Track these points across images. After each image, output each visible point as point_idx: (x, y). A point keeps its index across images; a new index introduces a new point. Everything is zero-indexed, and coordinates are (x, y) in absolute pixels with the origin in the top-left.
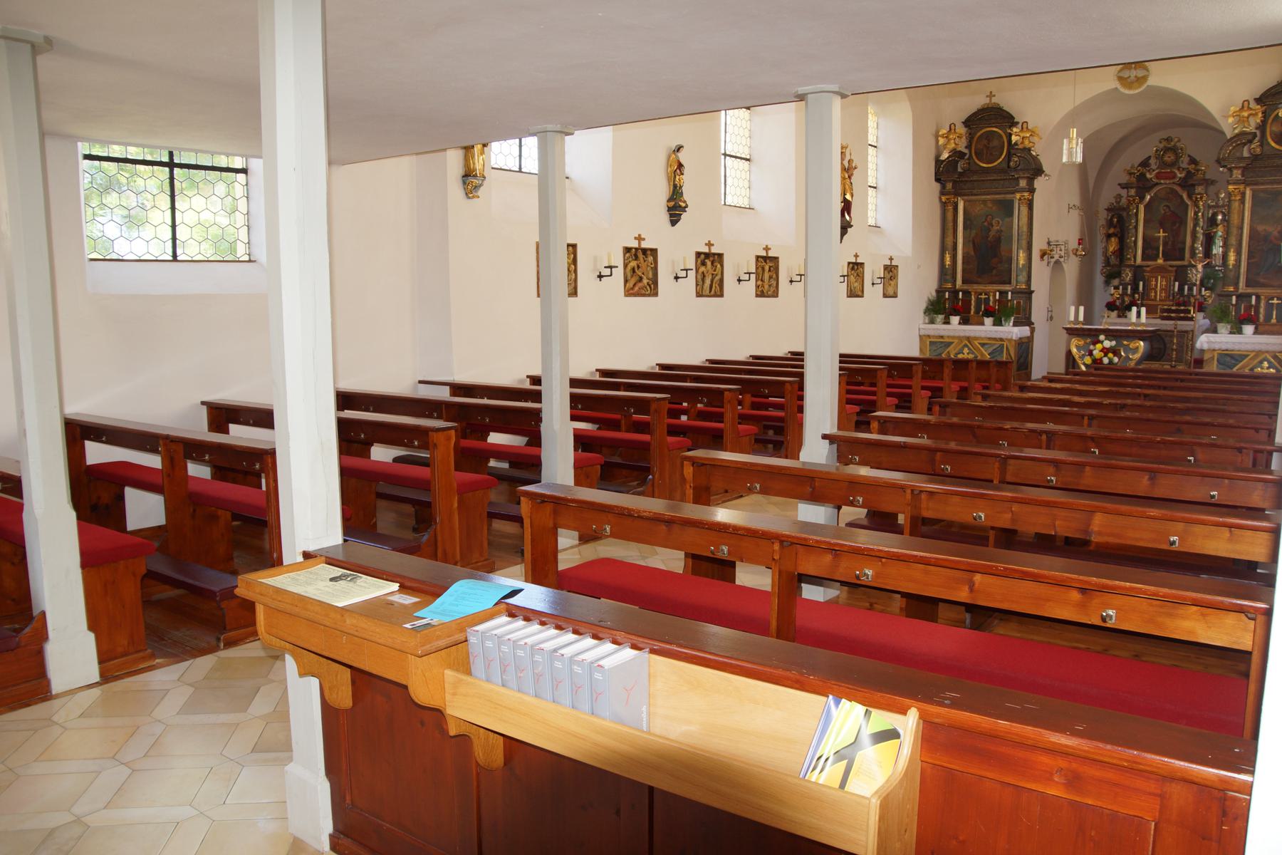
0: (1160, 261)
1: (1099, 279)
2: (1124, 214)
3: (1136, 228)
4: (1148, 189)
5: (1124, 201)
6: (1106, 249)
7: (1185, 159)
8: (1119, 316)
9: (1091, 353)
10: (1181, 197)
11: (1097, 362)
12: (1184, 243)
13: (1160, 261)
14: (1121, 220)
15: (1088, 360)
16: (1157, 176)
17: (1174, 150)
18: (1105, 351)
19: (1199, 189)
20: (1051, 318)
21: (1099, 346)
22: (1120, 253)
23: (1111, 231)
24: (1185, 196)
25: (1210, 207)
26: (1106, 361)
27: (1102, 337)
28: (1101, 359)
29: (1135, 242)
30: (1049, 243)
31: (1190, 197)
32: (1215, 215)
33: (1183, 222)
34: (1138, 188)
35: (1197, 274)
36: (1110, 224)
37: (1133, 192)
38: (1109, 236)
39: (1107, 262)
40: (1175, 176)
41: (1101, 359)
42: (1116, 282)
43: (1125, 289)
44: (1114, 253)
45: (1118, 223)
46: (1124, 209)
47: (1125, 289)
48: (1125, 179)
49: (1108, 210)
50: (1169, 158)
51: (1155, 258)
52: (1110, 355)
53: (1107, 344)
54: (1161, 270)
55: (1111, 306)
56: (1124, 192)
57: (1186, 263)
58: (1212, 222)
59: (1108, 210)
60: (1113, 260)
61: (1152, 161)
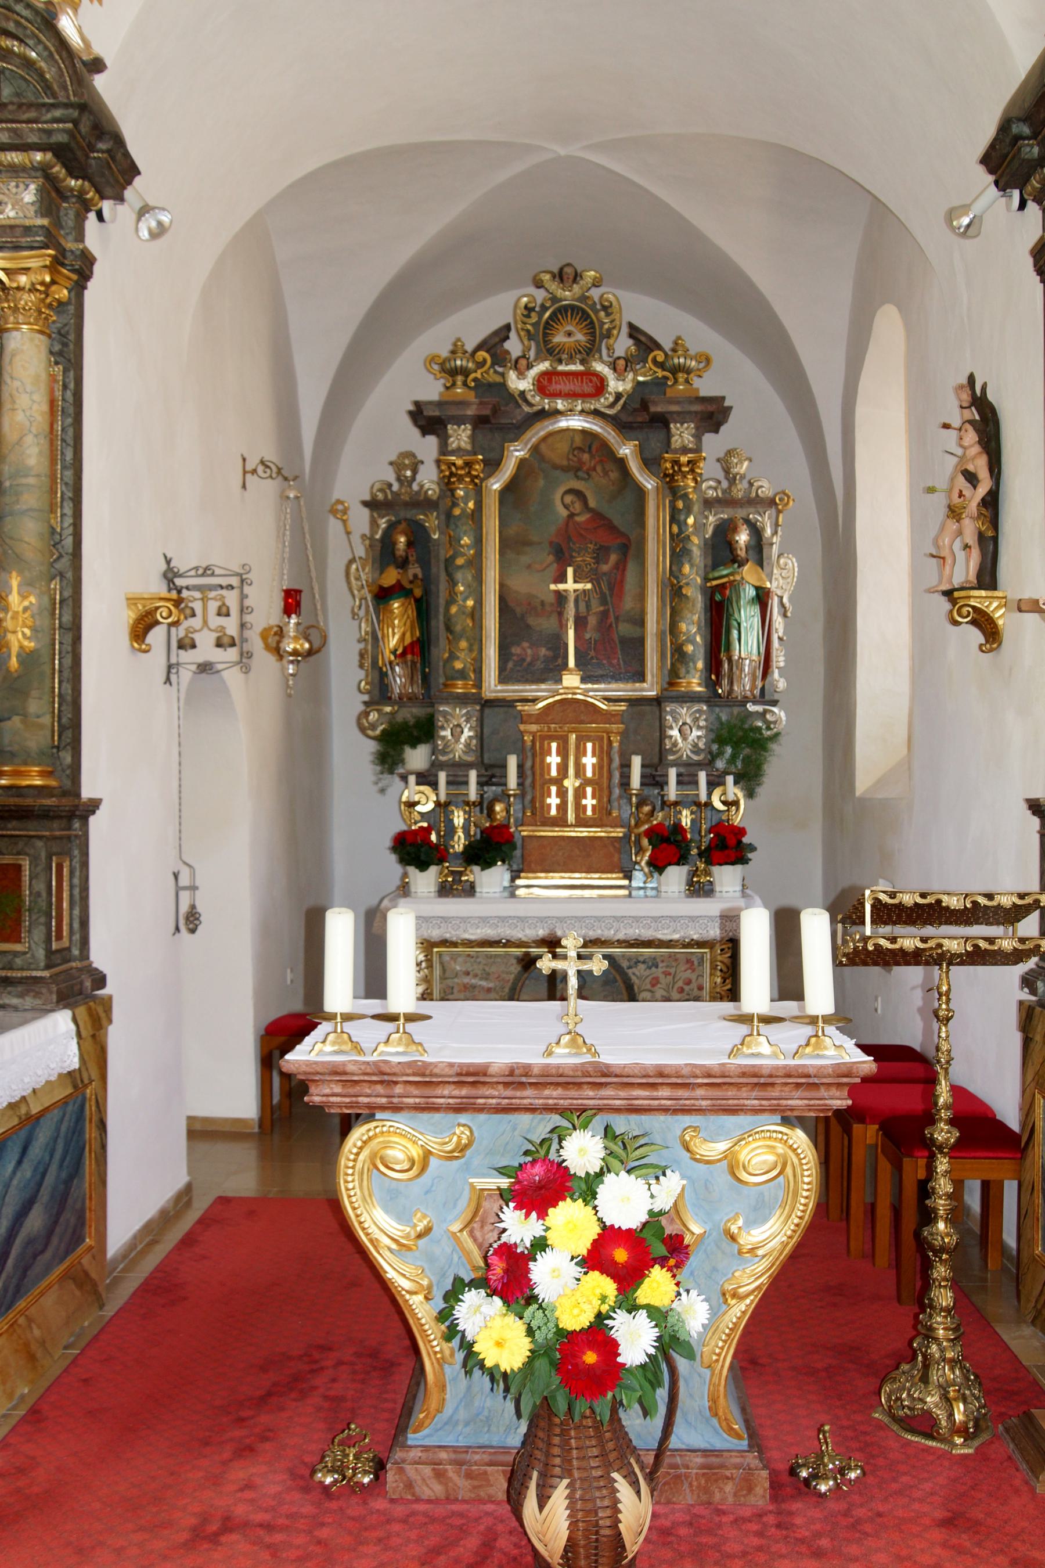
0: (571, 680)
1: (351, 752)
2: (431, 522)
3: (476, 564)
4: (517, 430)
5: (428, 479)
6: (376, 639)
7: (623, 345)
8: (444, 890)
9: (510, 1278)
10: (622, 464)
11: (581, 1361)
12: (641, 623)
13: (571, 680)
14: (418, 536)
15: (500, 1337)
16: (542, 385)
17: (580, 313)
18: (624, 1257)
19: (682, 434)
20: (192, 920)
21: (571, 1225)
22: (419, 651)
23: (391, 577)
24: (635, 467)
25: (709, 504)
26: (635, 1341)
27: (582, 1151)
28: (598, 1335)
29: (476, 614)
30: (170, 576)
31: (650, 463)
32: (724, 533)
33: (630, 548)
34: (480, 422)
35: (686, 732)
36: (384, 552)
37: (461, 436)
38: (382, 596)
39: (380, 691)
40: (600, 386)
41: (598, 1335)
42: (417, 758)
43: (457, 782)
44: (403, 654)
45: (409, 556)
46: (426, 504)
47: (457, 782)
48: (432, 390)
49: (371, 504)
50: (568, 335)
51: (554, 670)
52: (658, 1284)
53: (626, 1201)
54: (572, 711)
55: (414, 849)
56: (427, 447)
57: (649, 689)
58: (722, 549)
59: (371, 504)
60: (399, 679)
61: (514, 346)
